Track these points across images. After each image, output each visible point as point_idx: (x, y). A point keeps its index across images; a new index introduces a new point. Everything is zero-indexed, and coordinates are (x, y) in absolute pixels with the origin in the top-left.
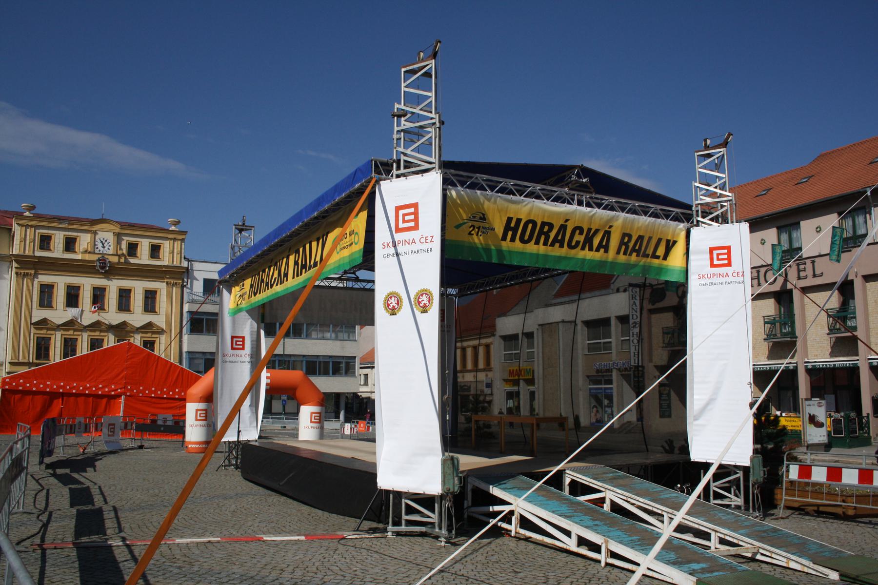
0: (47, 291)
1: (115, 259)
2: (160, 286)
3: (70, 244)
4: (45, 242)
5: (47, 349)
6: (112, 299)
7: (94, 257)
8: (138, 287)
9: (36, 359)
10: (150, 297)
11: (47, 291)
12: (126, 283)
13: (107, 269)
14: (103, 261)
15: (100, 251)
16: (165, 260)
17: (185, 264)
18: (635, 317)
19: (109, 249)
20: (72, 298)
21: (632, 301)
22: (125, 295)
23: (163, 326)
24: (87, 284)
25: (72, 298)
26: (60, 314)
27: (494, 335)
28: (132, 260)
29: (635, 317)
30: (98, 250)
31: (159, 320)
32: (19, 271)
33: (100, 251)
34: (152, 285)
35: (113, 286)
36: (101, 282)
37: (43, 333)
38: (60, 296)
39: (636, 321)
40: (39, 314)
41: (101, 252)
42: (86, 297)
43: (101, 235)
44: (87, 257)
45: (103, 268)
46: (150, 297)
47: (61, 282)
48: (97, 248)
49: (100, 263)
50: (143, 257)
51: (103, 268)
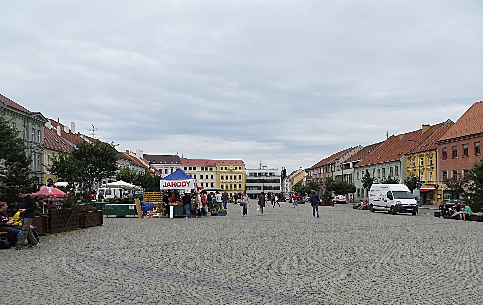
3: (226, 168)
4: (222, 168)
8: (237, 175)
10: (240, 177)
12: (235, 174)
24: (229, 175)
31: (241, 180)
35: (233, 175)
36: (231, 174)
37: (222, 184)
38: (225, 178)
40: (222, 181)
42: (229, 178)
46: (240, 177)
47: (225, 175)
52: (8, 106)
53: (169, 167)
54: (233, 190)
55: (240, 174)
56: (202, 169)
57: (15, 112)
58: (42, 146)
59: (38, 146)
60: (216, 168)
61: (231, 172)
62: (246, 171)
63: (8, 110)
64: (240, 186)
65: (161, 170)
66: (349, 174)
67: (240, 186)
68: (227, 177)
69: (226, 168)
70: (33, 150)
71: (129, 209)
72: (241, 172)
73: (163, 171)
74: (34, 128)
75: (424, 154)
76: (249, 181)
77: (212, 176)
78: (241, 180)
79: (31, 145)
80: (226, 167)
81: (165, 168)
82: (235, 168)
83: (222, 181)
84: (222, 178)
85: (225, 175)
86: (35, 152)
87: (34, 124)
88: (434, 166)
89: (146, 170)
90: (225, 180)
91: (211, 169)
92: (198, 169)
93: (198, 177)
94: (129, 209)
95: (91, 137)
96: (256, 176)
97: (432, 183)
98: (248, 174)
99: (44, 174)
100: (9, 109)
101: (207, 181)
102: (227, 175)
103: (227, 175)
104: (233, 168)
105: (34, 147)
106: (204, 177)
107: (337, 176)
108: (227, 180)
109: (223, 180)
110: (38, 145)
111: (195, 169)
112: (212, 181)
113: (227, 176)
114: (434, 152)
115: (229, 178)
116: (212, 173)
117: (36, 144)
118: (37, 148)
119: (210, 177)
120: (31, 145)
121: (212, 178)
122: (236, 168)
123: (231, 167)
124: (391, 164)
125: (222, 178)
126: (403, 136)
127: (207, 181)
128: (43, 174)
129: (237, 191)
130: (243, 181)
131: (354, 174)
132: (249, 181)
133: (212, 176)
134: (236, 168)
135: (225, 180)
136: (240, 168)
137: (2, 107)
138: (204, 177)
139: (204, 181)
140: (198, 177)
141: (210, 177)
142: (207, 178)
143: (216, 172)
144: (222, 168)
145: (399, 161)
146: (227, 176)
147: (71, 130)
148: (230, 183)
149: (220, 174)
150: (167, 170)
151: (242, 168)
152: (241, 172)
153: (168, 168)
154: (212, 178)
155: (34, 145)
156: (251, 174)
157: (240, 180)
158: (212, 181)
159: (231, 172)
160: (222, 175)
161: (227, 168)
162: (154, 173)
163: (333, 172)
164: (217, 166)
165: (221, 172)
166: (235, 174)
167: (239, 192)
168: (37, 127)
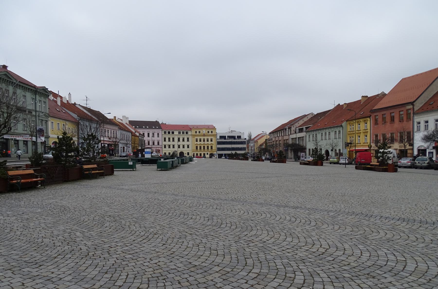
2: (212, 137)
3: (199, 132)
4: (196, 132)
7: (203, 134)
8: (210, 138)
12: (208, 137)
14: (204, 134)
17: (216, 134)
20: (200, 141)
23: (213, 143)
24: (202, 138)
25: (200, 141)
35: (206, 138)
37: (197, 146)
43: (203, 131)
47: (198, 138)
50: (210, 133)
52: (19, 82)
53: (151, 131)
54: (206, 150)
56: (179, 133)
57: (25, 87)
58: (47, 115)
59: (45, 115)
60: (191, 131)
61: (204, 135)
63: (20, 85)
64: (212, 147)
65: (144, 134)
66: (302, 137)
67: (212, 147)
69: (199, 132)
70: (40, 118)
71: (129, 164)
72: (213, 135)
73: (146, 135)
74: (41, 99)
75: (361, 120)
76: (219, 143)
77: (188, 139)
78: (213, 143)
79: (39, 114)
80: (199, 131)
81: (147, 132)
82: (207, 132)
83: (196, 143)
84: (197, 141)
85: (198, 138)
86: (42, 120)
87: (40, 96)
88: (369, 130)
89: (132, 134)
90: (199, 143)
91: (187, 133)
92: (176, 133)
93: (176, 140)
94: (129, 164)
95: (85, 106)
96: (225, 139)
97: (366, 144)
98: (218, 137)
99: (50, 138)
100: (20, 84)
101: (183, 143)
102: (200, 137)
103: (200, 137)
104: (206, 132)
105: (42, 115)
106: (181, 140)
107: (292, 139)
108: (200, 143)
109: (197, 143)
110: (44, 114)
111: (173, 133)
112: (188, 143)
114: (368, 119)
116: (188, 136)
117: (43, 113)
118: (44, 116)
119: (186, 140)
120: (39, 114)
121: (188, 141)
122: (208, 132)
123: (204, 131)
124: (322, 131)
126: (347, 105)
127: (183, 143)
128: (49, 138)
129: (210, 152)
130: (214, 143)
131: (306, 136)
132: (219, 143)
133: (188, 139)
134: (208, 132)
135: (199, 143)
136: (212, 132)
137: (15, 83)
138: (181, 140)
139: (181, 143)
140: (176, 140)
141: (186, 140)
142: (183, 140)
143: (192, 135)
144: (196, 132)
145: (342, 126)
147: (68, 100)
148: (203, 144)
149: (194, 137)
151: (213, 132)
152: (213, 135)
153: (150, 132)
154: (188, 141)
155: (41, 114)
156: (221, 137)
157: (212, 142)
158: (188, 143)
159: (204, 135)
160: (197, 138)
161: (201, 132)
162: (138, 137)
163: (289, 135)
164: (192, 131)
165: (195, 135)
166: (208, 137)
167: (211, 153)
168: (43, 99)
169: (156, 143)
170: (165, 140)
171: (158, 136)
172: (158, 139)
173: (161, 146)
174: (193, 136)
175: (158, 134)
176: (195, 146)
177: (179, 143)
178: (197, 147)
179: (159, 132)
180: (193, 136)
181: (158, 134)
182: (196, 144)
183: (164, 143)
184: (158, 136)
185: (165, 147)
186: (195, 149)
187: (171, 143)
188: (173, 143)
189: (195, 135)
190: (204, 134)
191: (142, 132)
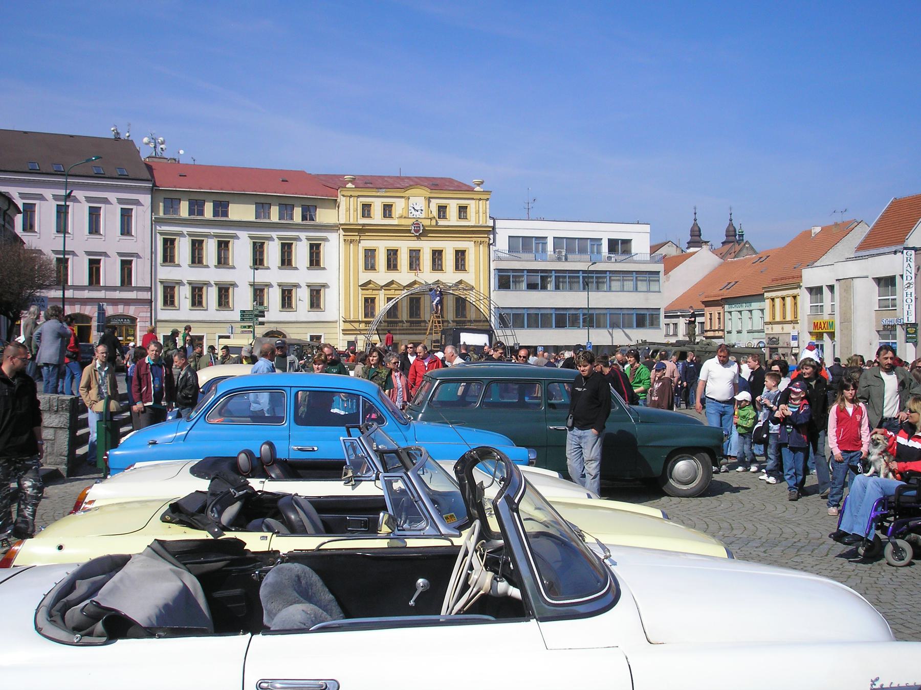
0: (370, 254)
1: (427, 222)
2: (468, 245)
3: (387, 210)
4: (366, 209)
5: (418, 308)
6: (426, 260)
7: (410, 222)
8: (449, 247)
9: (410, 318)
10: (460, 255)
11: (370, 254)
12: (437, 245)
13: (422, 233)
14: (417, 225)
15: (413, 215)
16: (472, 220)
17: (491, 223)
18: (909, 278)
19: (421, 213)
21: (906, 264)
22: (437, 255)
23: (473, 284)
24: (404, 246)
26: (382, 276)
27: (800, 287)
28: (442, 222)
29: (909, 278)
30: (412, 214)
31: (468, 277)
32: (347, 238)
33: (413, 215)
34: (461, 245)
35: (426, 247)
36: (415, 244)
37: (369, 294)
38: (381, 260)
39: (910, 282)
40: (365, 277)
41: (415, 216)
42: (403, 260)
44: (404, 222)
45: (417, 231)
46: (460, 255)
47: (381, 246)
48: (411, 213)
49: (415, 227)
50: (452, 219)
51: (417, 231)
55: (461, 245)
62: (494, 228)
68: (392, 255)
82: (435, 213)
84: (370, 265)
98: (502, 243)
102: (393, 244)
103: (393, 244)
108: (392, 276)
112: (316, 277)
113: (395, 252)
115: (403, 260)
121: (315, 261)
125: (370, 265)
132: (505, 281)
134: (442, 209)
135: (382, 276)
144: (366, 209)
146: (395, 252)
150: (66, 213)
151: (471, 212)
154: (315, 261)
165: (363, 231)
166: (437, 245)
169: (110, 273)
170: (169, 258)
171: (126, 230)
172: (128, 245)
173: (146, 295)
174: (355, 232)
175: (126, 215)
176: (362, 295)
177: (262, 276)
178: (369, 303)
179: (137, 203)
180: (355, 232)
181: (126, 215)
182: (365, 286)
183: (166, 273)
184: (126, 230)
185: (169, 300)
186: (361, 317)
187: (211, 274)
188: (224, 275)
189: (363, 231)
190: (417, 225)
191: (23, 196)
